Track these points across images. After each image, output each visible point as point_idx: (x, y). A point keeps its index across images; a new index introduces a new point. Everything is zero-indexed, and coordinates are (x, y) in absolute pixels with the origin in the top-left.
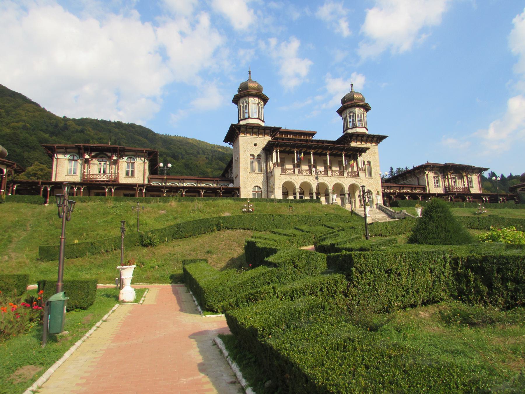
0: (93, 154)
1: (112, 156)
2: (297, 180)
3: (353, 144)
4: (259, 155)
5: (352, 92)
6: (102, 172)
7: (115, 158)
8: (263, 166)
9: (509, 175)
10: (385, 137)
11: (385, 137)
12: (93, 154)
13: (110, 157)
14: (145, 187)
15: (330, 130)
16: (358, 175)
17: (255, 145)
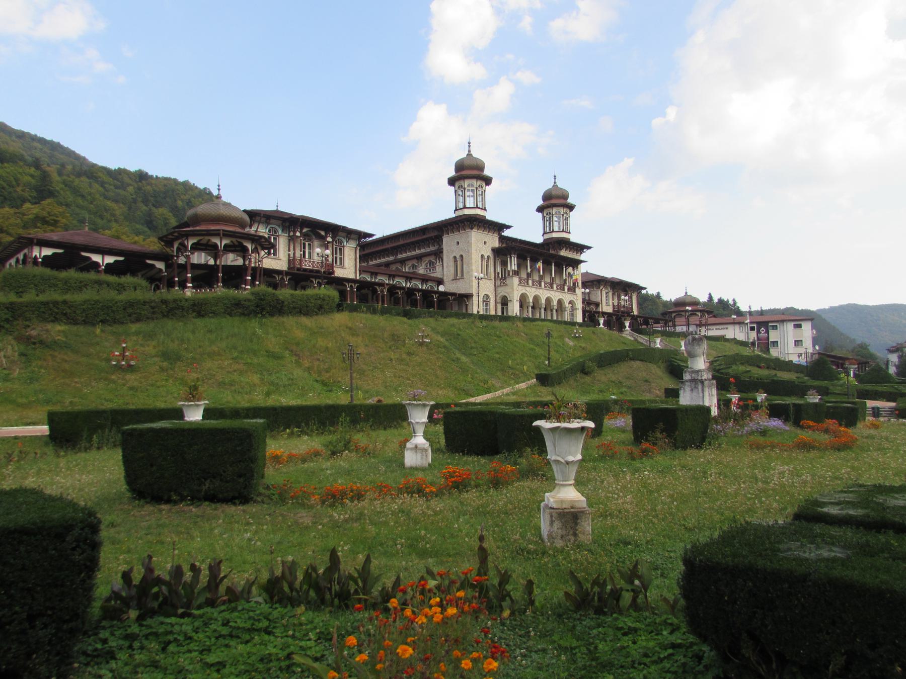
0: (305, 230)
1: (327, 237)
2: (531, 292)
3: (563, 253)
4: (488, 257)
5: (555, 186)
6: (307, 256)
7: (329, 239)
8: (492, 269)
9: (655, 293)
10: (589, 248)
11: (589, 248)
12: (305, 230)
13: (323, 238)
14: (387, 287)
15: (529, 229)
16: (574, 291)
17: (485, 243)
